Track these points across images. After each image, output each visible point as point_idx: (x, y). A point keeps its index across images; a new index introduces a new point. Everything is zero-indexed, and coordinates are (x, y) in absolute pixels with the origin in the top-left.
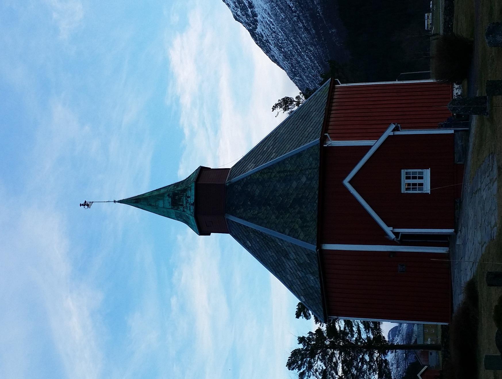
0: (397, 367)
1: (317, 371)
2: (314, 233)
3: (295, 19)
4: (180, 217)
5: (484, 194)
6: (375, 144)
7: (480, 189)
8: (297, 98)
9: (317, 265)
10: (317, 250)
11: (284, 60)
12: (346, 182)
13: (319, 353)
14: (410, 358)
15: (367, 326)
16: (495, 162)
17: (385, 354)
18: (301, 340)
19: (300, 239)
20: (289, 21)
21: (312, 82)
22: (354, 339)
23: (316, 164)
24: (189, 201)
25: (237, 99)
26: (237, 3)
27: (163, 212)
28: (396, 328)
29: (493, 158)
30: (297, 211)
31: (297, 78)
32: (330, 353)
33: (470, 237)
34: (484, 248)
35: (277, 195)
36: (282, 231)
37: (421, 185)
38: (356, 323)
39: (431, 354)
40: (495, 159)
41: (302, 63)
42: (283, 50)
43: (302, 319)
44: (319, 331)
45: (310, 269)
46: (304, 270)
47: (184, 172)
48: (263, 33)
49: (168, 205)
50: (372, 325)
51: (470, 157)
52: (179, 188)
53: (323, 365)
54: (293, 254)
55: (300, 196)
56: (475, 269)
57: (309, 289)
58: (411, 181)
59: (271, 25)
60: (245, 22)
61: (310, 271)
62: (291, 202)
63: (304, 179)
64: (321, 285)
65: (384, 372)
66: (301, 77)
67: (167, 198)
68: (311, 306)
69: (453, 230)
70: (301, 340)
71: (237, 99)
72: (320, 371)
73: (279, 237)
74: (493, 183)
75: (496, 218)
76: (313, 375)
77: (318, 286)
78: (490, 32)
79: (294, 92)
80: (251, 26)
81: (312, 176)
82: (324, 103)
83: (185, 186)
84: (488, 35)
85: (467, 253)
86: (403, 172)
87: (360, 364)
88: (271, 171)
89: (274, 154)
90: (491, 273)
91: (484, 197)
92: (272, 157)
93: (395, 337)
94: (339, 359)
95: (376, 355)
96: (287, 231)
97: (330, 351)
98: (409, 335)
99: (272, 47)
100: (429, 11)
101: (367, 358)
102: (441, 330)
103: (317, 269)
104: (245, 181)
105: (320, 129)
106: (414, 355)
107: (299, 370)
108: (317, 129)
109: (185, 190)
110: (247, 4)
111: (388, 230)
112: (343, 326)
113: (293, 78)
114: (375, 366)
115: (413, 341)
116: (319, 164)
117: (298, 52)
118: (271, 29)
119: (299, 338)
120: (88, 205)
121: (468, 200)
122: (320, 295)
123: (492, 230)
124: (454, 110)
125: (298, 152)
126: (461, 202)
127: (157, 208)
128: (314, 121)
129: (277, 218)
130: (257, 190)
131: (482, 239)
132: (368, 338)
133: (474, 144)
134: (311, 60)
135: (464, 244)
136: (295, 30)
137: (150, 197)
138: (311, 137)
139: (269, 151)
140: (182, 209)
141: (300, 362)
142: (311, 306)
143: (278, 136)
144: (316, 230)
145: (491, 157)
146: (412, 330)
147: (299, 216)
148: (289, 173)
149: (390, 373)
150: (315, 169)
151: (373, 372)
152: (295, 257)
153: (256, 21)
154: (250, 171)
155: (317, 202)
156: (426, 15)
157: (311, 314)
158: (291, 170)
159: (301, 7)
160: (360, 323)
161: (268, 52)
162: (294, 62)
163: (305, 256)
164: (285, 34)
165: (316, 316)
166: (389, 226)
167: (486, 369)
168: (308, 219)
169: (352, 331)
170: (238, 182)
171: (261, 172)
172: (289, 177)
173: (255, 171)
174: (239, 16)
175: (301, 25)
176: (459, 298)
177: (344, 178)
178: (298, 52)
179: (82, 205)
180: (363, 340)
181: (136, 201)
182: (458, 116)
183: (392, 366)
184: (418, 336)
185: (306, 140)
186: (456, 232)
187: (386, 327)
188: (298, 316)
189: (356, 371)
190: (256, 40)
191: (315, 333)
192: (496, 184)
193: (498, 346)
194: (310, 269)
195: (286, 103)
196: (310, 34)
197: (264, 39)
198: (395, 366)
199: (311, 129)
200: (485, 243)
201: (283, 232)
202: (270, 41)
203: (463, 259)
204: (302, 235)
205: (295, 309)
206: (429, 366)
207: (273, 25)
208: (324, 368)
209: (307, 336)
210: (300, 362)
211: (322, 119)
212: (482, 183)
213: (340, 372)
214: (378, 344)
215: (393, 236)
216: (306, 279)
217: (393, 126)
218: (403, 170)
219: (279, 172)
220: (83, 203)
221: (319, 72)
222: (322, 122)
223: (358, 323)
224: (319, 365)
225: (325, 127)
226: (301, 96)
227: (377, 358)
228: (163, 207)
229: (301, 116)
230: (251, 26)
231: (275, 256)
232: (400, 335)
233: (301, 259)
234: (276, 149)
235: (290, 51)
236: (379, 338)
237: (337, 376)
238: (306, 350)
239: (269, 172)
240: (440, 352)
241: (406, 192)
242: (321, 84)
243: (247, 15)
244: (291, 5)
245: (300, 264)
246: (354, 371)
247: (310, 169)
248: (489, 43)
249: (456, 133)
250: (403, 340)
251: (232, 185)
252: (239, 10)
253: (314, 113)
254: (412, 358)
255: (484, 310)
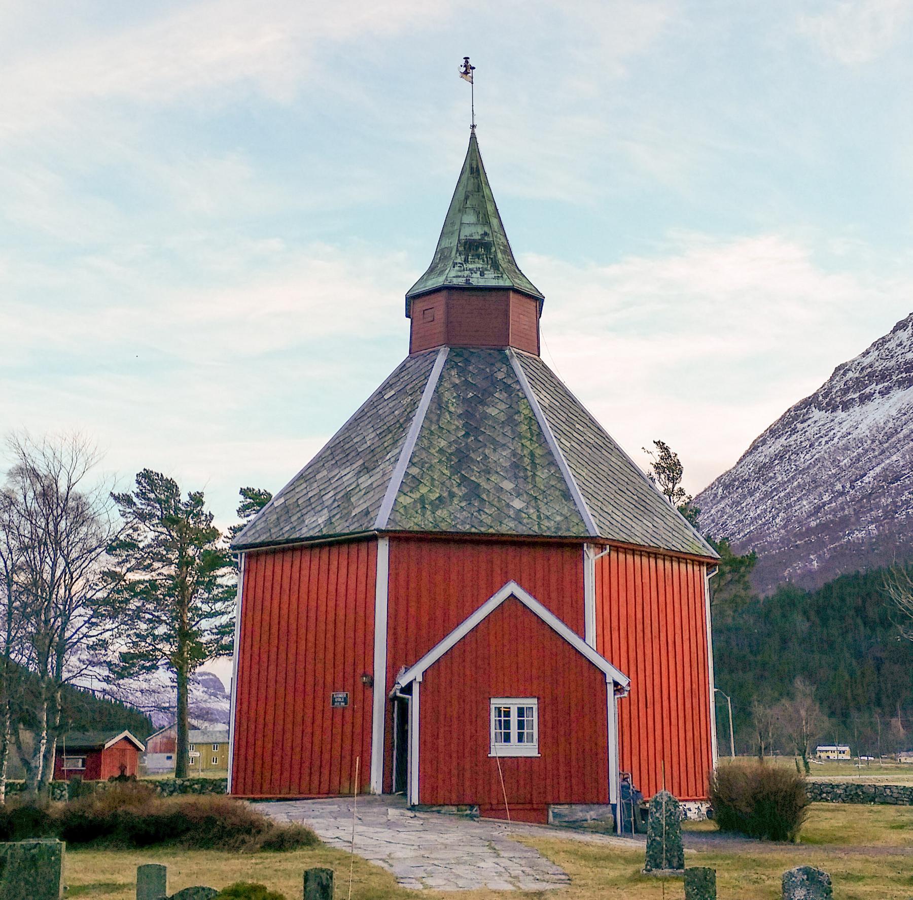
0: (142, 691)
1: (135, 530)
2: (411, 524)
3: (839, 487)
4: (442, 256)
5: (489, 864)
6: (588, 646)
7: (498, 856)
8: (681, 490)
9: (346, 531)
10: (377, 530)
11: (755, 464)
12: (513, 588)
13: (170, 536)
14: (161, 715)
15: (223, 631)
16: (552, 886)
17: (169, 666)
18: (197, 499)
19: (398, 496)
20: (835, 475)
21: (713, 521)
22: (199, 605)
23: (549, 528)
24: (474, 275)
25: (681, 370)
26: (869, 370)
27: (453, 224)
28: (221, 688)
29: (561, 881)
30: (455, 490)
31: (720, 490)
32: (170, 556)
33: (402, 835)
34: (381, 863)
35: (487, 451)
36: (415, 460)
37: (507, 738)
38: (230, 609)
39: (169, 758)
40: (558, 886)
41: (749, 500)
42: (777, 462)
43: (239, 500)
44: (214, 534)
45: (338, 516)
46: (336, 504)
47: (534, 265)
48: (809, 422)
49: (466, 232)
50: (226, 640)
51: (563, 835)
52: (500, 255)
53: (146, 542)
54: (369, 482)
55: (484, 496)
56: (339, 845)
57: (299, 515)
58: (514, 719)
59: (826, 439)
60: (833, 387)
61: (334, 516)
62: (473, 478)
63: (518, 504)
64: (307, 539)
65: (133, 665)
66: (722, 498)
67: (481, 232)
68: (264, 519)
69: (417, 803)
70: (197, 499)
71: (681, 370)
72: (135, 537)
73: (402, 454)
74: (511, 883)
75: (441, 888)
76: (127, 523)
77: (305, 532)
78: (812, 877)
79: (692, 484)
80: (825, 398)
81: (525, 521)
82: (670, 545)
83: (504, 266)
84: (806, 871)
85: (371, 830)
86: (532, 703)
87: (148, 616)
88: (534, 439)
89: (568, 445)
90: (331, 877)
91: (482, 864)
92: (563, 440)
93: (203, 685)
94: (158, 575)
95: (167, 648)
96: (415, 471)
97: (174, 556)
98: (206, 715)
99: (782, 440)
100: (854, 754)
101: (162, 630)
102: (217, 778)
103: (338, 530)
104: (514, 386)
105: (617, 537)
106: (166, 724)
107: (137, 495)
108: (617, 530)
109: (496, 266)
110: (868, 390)
111: (415, 673)
112: (225, 583)
113: (719, 483)
114: (144, 647)
115: (194, 722)
116: (548, 534)
117: (772, 492)
118: (818, 438)
119: (201, 495)
120: (466, 73)
121: (477, 831)
122: (286, 536)
123: (416, 879)
124: (658, 804)
125: (572, 492)
126: (472, 817)
127: (459, 210)
128: (634, 525)
129: (441, 451)
130: (497, 411)
131: (399, 859)
132: (200, 633)
133: (587, 844)
134: (756, 518)
135: (389, 825)
136: (816, 487)
137: (483, 197)
138: (602, 519)
139: (575, 434)
140: (459, 261)
141: (152, 496)
142: (264, 519)
143: (604, 452)
144: (416, 528)
145: (563, 877)
146: (217, 721)
147: (445, 494)
148: (530, 474)
149: (131, 676)
150: (540, 528)
151: (133, 642)
152: (362, 487)
153: (834, 410)
154: (533, 397)
155: (473, 530)
156: (847, 748)
157: (249, 518)
158: (537, 479)
159: (862, 499)
160: (230, 616)
161: (773, 432)
162: (752, 485)
163: (364, 506)
164: (808, 467)
165: (245, 529)
166: (425, 673)
167: (139, 868)
168: (439, 512)
169: (216, 600)
170: (511, 372)
171: (532, 419)
172: (522, 474)
173: (533, 405)
174: (844, 374)
175: (826, 498)
176: (280, 815)
177: (520, 584)
178: (772, 492)
179: (467, 62)
180: (198, 622)
181: (474, 169)
182: (645, 813)
183: (146, 680)
184: (204, 733)
185: (596, 508)
186: (413, 808)
187: (223, 669)
188: (244, 492)
189: (134, 608)
190: (797, 408)
191: (212, 525)
192: (509, 887)
193: (183, 894)
194: (338, 516)
195: (670, 467)
196: (808, 517)
197: (799, 425)
198: (145, 686)
199: (619, 519)
200: (391, 866)
201: (412, 463)
202: (794, 437)
203: (359, 822)
204: (406, 500)
205: (258, 485)
206: (145, 754)
207: (827, 442)
208: (141, 545)
209: (205, 509)
210: (152, 496)
211: (639, 540)
212: (510, 859)
213: (132, 577)
214: (188, 652)
215: (403, 681)
216: (319, 508)
217: (623, 681)
218: (535, 701)
219: (532, 454)
220: (471, 63)
221: (733, 534)
222: (631, 541)
223: (234, 611)
224: (147, 535)
225: (620, 547)
226: (683, 498)
227: (160, 650)
228: (461, 224)
229: (644, 498)
230: (825, 398)
231: (365, 446)
232: (207, 697)
233: (359, 499)
234: (579, 448)
235: (775, 477)
236: (200, 654)
237: (124, 570)
238: (177, 509)
239: (532, 434)
240: (172, 776)
241: (493, 707)
242: (708, 539)
243: (845, 391)
244: (866, 479)
245: (347, 496)
246: (135, 603)
247: (539, 517)
248: (791, 875)
249: (610, 807)
250: (197, 702)
251: (506, 360)
252: (857, 375)
253: (650, 525)
254: (160, 719)
255: (257, 864)
